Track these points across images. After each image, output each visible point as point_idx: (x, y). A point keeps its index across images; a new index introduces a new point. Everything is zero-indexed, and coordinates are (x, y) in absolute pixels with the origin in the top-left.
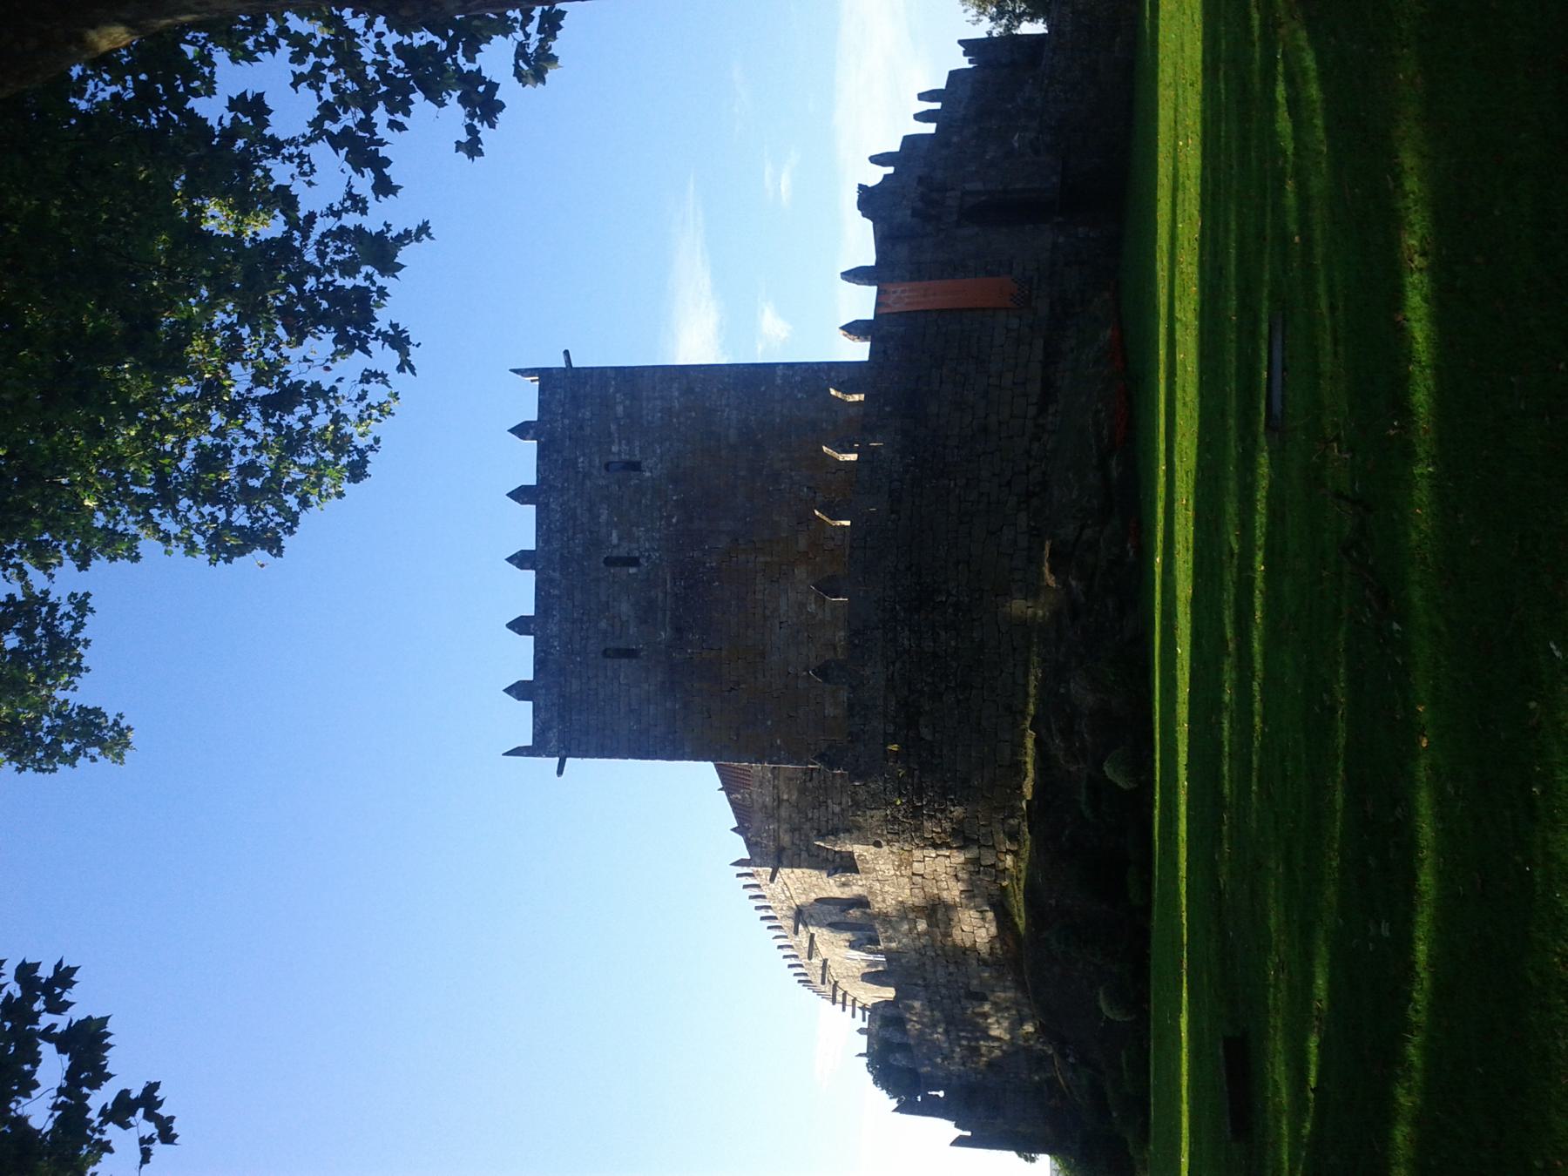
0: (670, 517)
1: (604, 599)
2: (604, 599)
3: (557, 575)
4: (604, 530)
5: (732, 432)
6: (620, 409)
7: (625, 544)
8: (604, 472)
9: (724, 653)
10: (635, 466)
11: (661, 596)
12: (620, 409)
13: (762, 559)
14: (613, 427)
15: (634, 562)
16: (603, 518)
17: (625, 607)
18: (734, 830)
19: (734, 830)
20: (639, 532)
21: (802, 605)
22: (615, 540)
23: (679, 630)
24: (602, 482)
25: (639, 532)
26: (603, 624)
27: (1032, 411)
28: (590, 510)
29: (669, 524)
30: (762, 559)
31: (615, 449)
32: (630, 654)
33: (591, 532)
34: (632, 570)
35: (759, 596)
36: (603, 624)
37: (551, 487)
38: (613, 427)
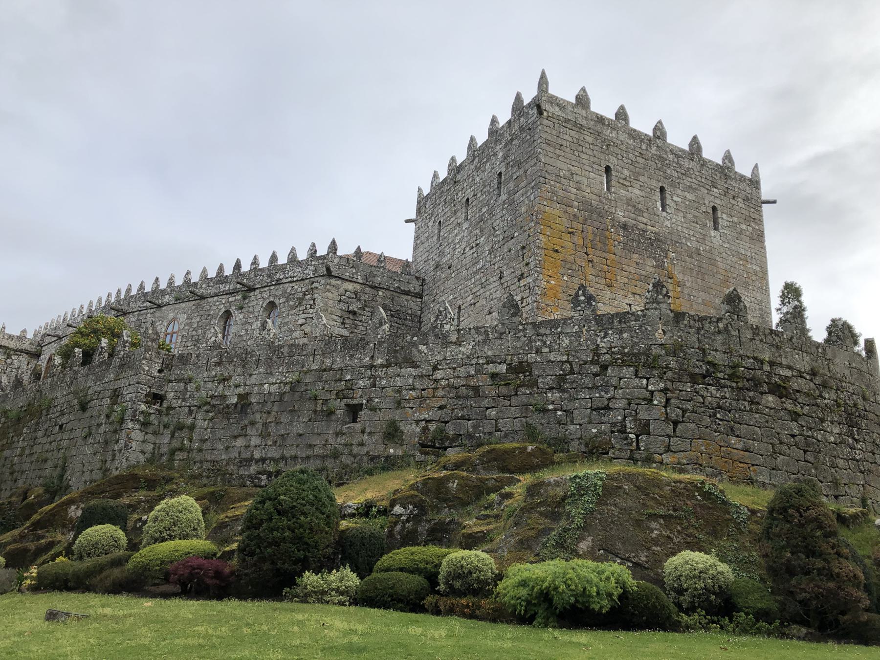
1: (641, 178)
6: (744, 227)
7: (673, 205)
8: (712, 204)
10: (716, 228)
11: (645, 220)
12: (744, 227)
14: (735, 219)
15: (664, 206)
18: (359, 248)
19: (359, 248)
22: (675, 198)
23: (625, 227)
33: (679, 183)
36: (626, 172)
37: (702, 165)
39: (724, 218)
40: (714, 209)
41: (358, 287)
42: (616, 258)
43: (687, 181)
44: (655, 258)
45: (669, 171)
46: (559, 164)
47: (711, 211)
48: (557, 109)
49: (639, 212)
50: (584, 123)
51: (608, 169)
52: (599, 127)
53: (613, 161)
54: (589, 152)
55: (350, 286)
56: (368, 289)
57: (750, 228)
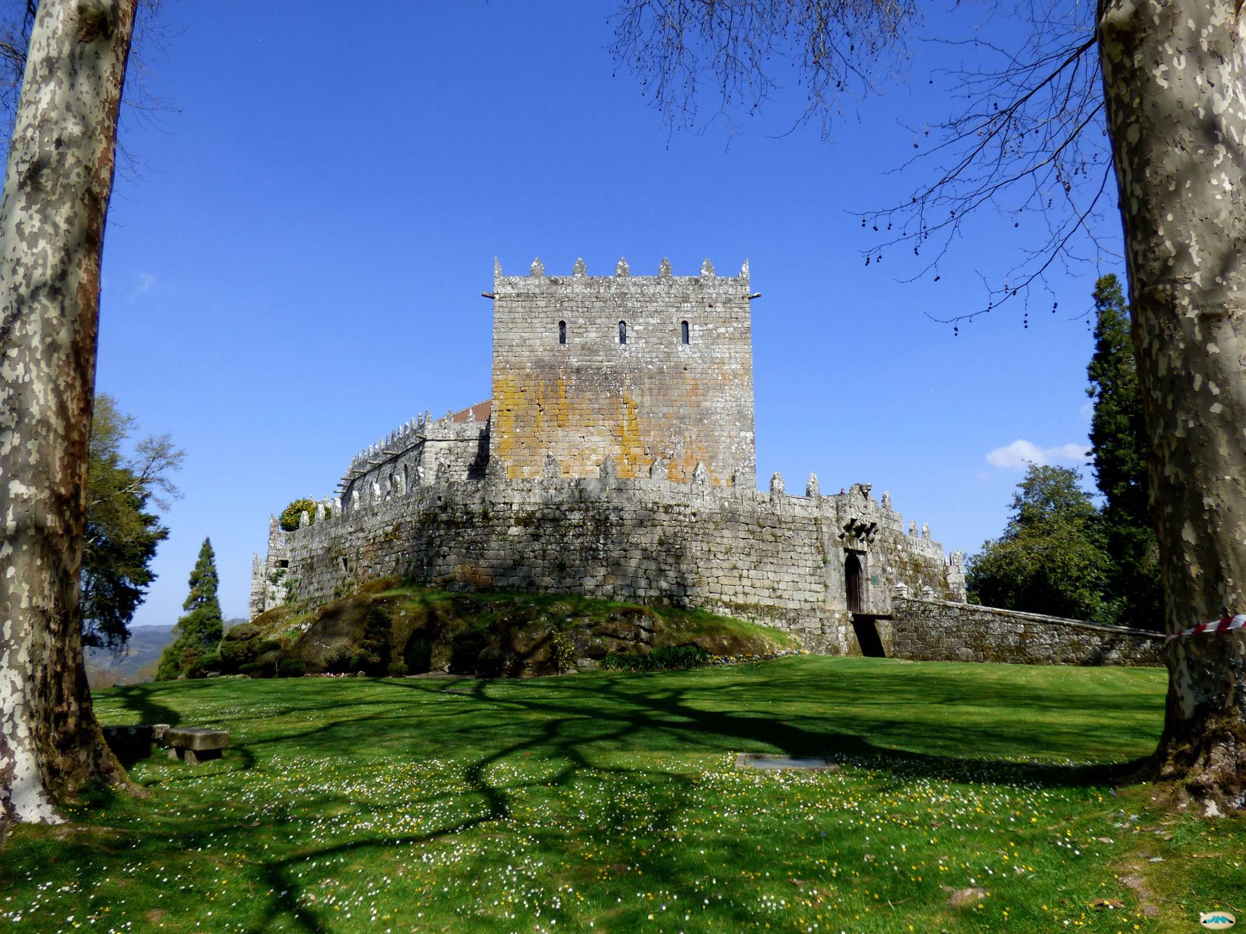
0: (651, 363)
1: (598, 321)
2: (598, 321)
3: (613, 290)
4: (641, 320)
5: (708, 404)
6: (722, 330)
7: (634, 334)
9: (563, 400)
10: (686, 339)
11: (600, 358)
12: (722, 330)
13: (625, 423)
14: (710, 326)
15: (623, 339)
16: (651, 321)
17: (593, 335)
20: (642, 343)
21: (594, 451)
22: (636, 328)
23: (578, 371)
24: (674, 320)
25: (642, 343)
26: (581, 321)
27: (726, 598)
28: (656, 311)
29: (647, 363)
30: (625, 423)
31: (696, 327)
32: (563, 340)
34: (617, 340)
35: (601, 422)
36: (581, 321)
37: (671, 286)
38: (710, 326)
39: (695, 330)
40: (685, 323)
41: (452, 443)
42: (567, 401)
43: (652, 307)
44: (609, 391)
45: (630, 305)
46: (512, 336)
47: (680, 328)
48: (509, 288)
49: (594, 352)
50: (537, 291)
51: (562, 324)
52: (553, 289)
53: (567, 316)
54: (542, 315)
55: (444, 445)
56: (460, 444)
57: (731, 330)
